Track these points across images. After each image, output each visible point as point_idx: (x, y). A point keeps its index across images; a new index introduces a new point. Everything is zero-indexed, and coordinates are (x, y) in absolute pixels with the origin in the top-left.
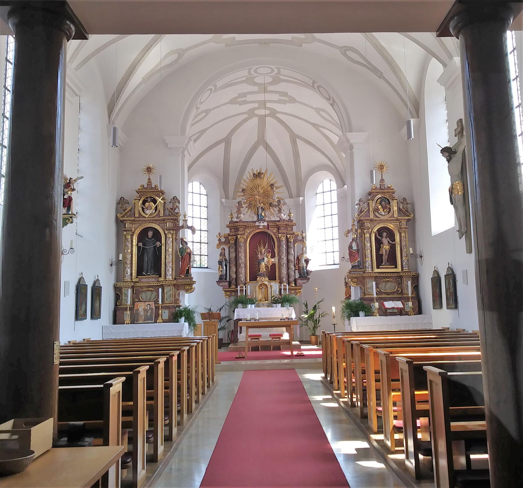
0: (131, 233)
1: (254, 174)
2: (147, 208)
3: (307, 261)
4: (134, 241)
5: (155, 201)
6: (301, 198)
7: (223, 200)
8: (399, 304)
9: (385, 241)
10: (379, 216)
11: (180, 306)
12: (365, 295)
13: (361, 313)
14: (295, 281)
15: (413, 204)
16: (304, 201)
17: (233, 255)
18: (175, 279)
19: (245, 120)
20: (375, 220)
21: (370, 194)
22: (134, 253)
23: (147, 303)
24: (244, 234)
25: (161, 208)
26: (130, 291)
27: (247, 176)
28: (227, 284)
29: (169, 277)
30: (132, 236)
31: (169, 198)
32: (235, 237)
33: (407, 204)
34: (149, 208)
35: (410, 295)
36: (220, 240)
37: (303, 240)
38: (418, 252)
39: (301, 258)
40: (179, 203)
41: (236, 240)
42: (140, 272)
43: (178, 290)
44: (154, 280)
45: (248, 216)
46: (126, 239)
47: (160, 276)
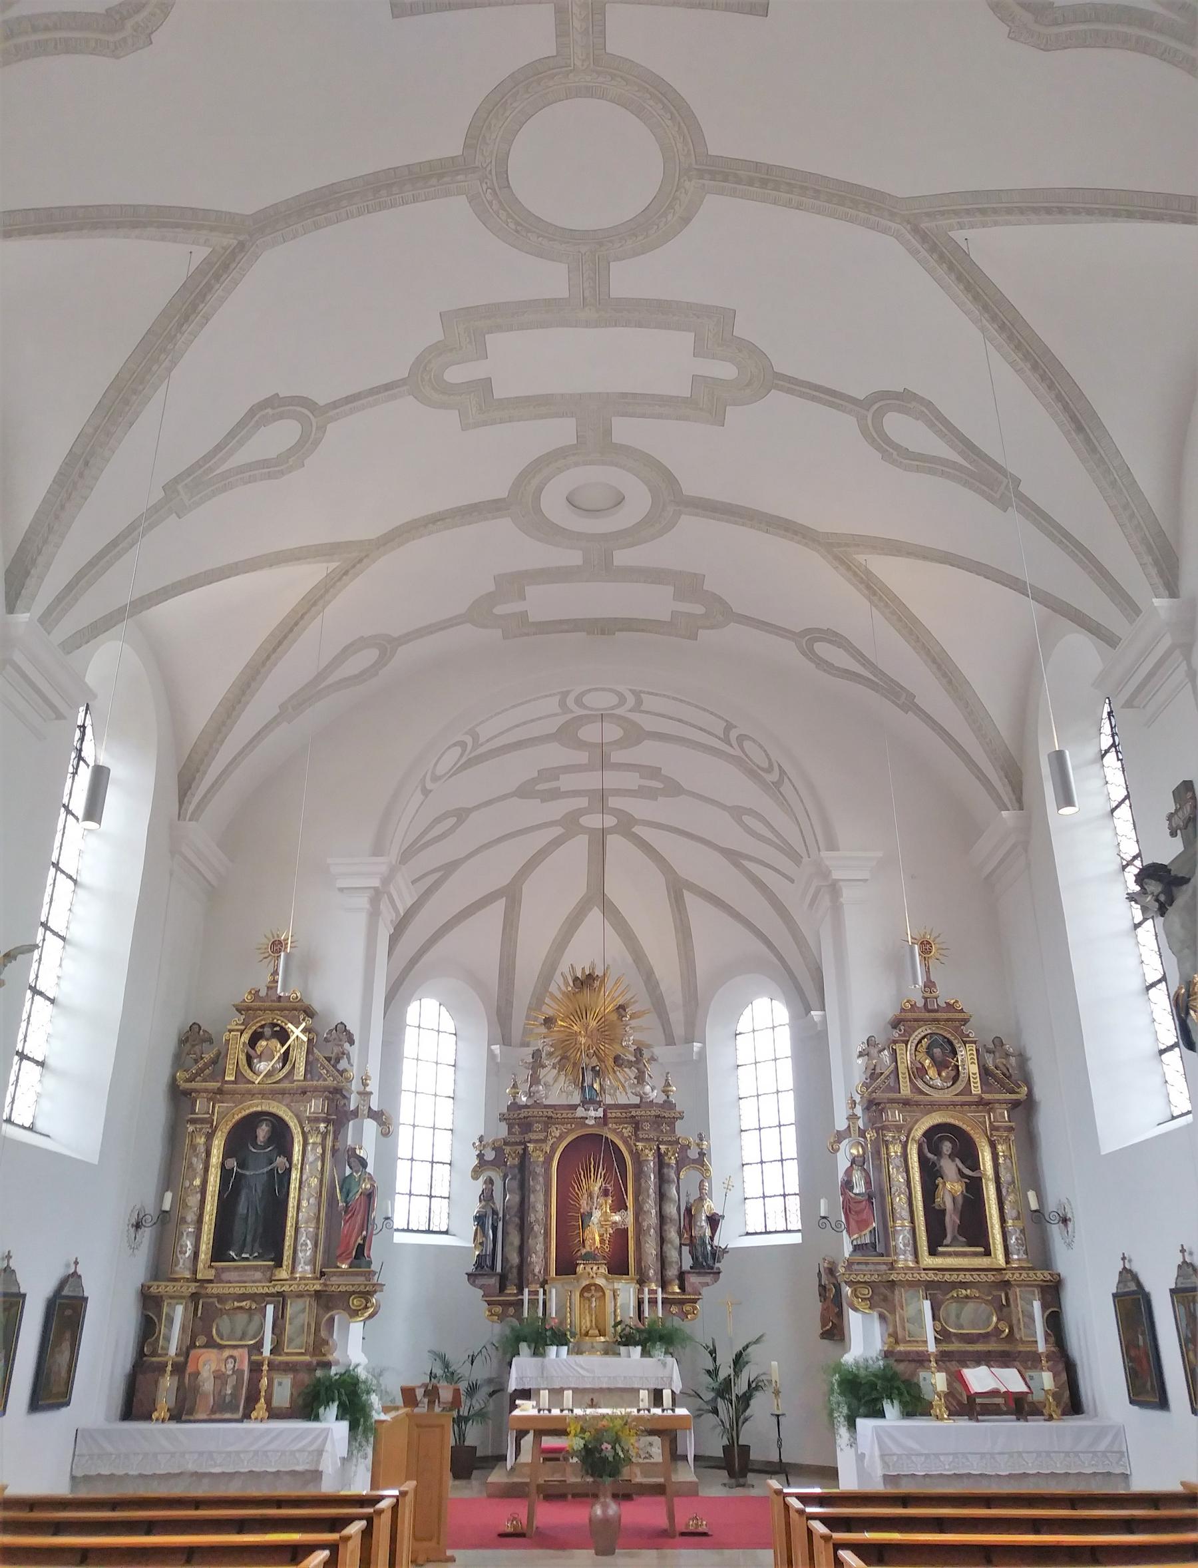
0: (206, 1128)
1: (576, 979)
2: (260, 1056)
3: (714, 1221)
4: (215, 1152)
5: (283, 1036)
7: (496, 1048)
8: (1011, 1380)
9: (949, 1167)
10: (926, 1089)
11: (328, 1365)
12: (897, 1342)
13: (891, 1410)
14: (682, 1276)
15: (1023, 1059)
16: (702, 1054)
18: (322, 1274)
19: (557, 843)
20: (917, 1104)
21: (896, 1024)
22: (210, 1188)
23: (227, 1353)
24: (544, 1141)
25: (299, 1058)
26: (180, 1309)
27: (559, 985)
28: (493, 1281)
29: (304, 1269)
30: (210, 1137)
33: (1007, 1055)
34: (267, 1055)
35: (1041, 1347)
36: (480, 1156)
37: (701, 1161)
38: (1052, 1205)
39: (699, 1211)
40: (352, 1042)
41: (524, 1156)
42: (219, 1253)
43: (328, 1308)
44: (258, 1275)
46: (194, 1147)
47: (279, 1264)
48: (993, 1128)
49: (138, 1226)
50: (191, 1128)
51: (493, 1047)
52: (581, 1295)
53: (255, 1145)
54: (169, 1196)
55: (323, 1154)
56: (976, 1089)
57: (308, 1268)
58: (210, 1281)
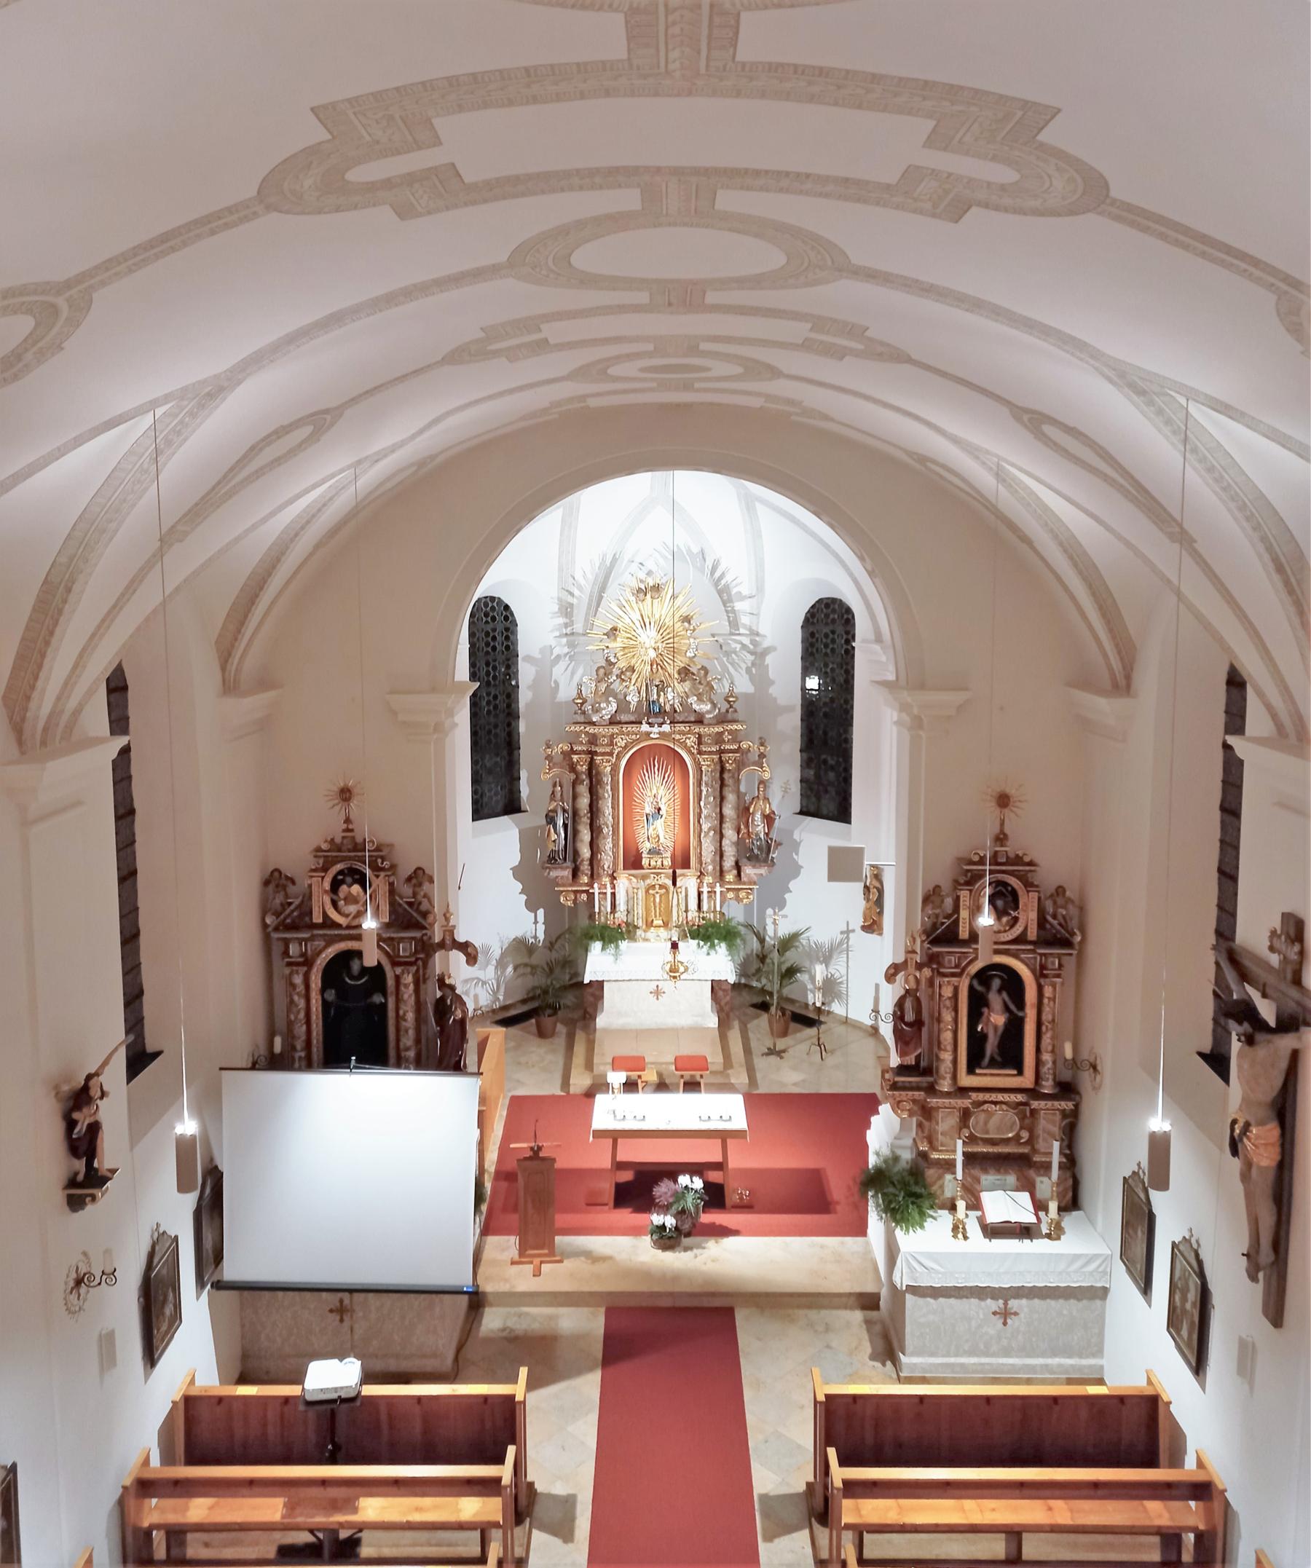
9: (996, 999)
15: (1082, 909)
24: (611, 754)
31: (406, 869)
38: (1085, 1055)
40: (431, 880)
41: (591, 764)
52: (647, 891)
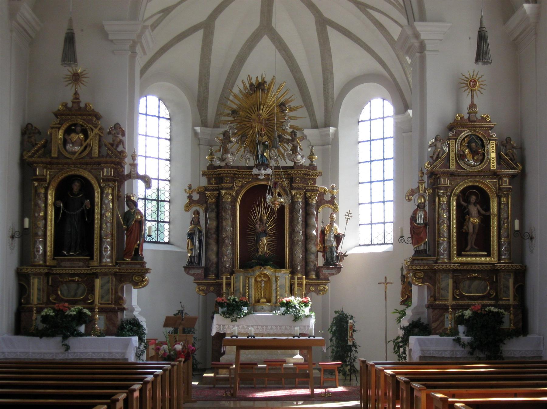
1: (251, 85)
3: (339, 238)
4: (50, 197)
6: (332, 129)
7: (198, 129)
9: (474, 210)
11: (123, 310)
12: (435, 300)
14: (318, 271)
15: (522, 149)
16: (336, 134)
17: (213, 224)
18: (117, 264)
21: (451, 128)
22: (49, 217)
24: (231, 188)
27: (238, 87)
28: (200, 271)
30: (47, 189)
32: (216, 193)
33: (513, 147)
35: (511, 302)
36: (190, 197)
37: (332, 202)
38: (527, 230)
41: (219, 198)
42: (57, 251)
44: (81, 264)
45: (238, 157)
46: (37, 194)
47: (92, 258)
48: (500, 189)
49: (13, 237)
50: (36, 184)
51: (196, 128)
52: (256, 280)
53: (73, 194)
54: (27, 221)
55: (113, 199)
56: (493, 166)
57: (108, 260)
58: (55, 267)
